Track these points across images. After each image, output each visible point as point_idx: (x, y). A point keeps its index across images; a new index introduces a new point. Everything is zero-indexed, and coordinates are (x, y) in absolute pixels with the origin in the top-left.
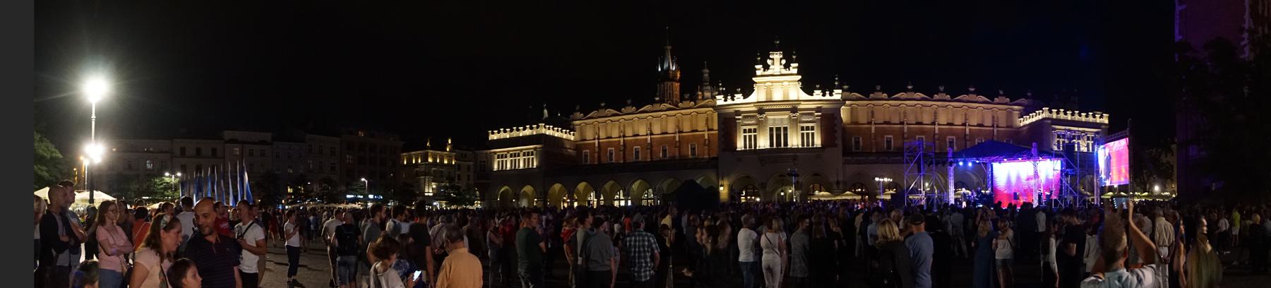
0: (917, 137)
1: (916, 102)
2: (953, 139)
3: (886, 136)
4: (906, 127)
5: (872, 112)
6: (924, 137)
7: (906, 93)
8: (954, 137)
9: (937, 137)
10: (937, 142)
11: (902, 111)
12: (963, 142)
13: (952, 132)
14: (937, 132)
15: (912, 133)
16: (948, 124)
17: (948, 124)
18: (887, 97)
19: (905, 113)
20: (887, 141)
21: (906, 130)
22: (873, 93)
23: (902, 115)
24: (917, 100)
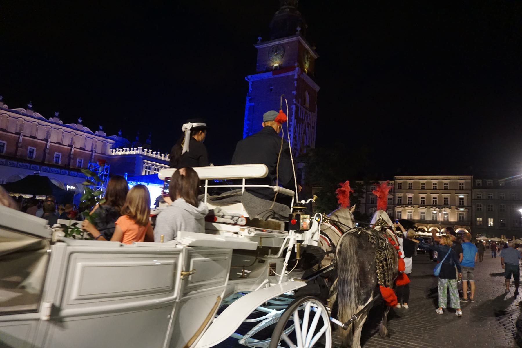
0: (29, 147)
6: (35, 149)
7: (26, 109)
9: (47, 151)
10: (47, 155)
11: (19, 123)
12: (67, 159)
13: (59, 150)
14: (48, 147)
15: (26, 144)
16: (57, 143)
17: (57, 143)
18: (7, 108)
19: (21, 125)
21: (21, 140)
23: (19, 126)
24: (35, 118)
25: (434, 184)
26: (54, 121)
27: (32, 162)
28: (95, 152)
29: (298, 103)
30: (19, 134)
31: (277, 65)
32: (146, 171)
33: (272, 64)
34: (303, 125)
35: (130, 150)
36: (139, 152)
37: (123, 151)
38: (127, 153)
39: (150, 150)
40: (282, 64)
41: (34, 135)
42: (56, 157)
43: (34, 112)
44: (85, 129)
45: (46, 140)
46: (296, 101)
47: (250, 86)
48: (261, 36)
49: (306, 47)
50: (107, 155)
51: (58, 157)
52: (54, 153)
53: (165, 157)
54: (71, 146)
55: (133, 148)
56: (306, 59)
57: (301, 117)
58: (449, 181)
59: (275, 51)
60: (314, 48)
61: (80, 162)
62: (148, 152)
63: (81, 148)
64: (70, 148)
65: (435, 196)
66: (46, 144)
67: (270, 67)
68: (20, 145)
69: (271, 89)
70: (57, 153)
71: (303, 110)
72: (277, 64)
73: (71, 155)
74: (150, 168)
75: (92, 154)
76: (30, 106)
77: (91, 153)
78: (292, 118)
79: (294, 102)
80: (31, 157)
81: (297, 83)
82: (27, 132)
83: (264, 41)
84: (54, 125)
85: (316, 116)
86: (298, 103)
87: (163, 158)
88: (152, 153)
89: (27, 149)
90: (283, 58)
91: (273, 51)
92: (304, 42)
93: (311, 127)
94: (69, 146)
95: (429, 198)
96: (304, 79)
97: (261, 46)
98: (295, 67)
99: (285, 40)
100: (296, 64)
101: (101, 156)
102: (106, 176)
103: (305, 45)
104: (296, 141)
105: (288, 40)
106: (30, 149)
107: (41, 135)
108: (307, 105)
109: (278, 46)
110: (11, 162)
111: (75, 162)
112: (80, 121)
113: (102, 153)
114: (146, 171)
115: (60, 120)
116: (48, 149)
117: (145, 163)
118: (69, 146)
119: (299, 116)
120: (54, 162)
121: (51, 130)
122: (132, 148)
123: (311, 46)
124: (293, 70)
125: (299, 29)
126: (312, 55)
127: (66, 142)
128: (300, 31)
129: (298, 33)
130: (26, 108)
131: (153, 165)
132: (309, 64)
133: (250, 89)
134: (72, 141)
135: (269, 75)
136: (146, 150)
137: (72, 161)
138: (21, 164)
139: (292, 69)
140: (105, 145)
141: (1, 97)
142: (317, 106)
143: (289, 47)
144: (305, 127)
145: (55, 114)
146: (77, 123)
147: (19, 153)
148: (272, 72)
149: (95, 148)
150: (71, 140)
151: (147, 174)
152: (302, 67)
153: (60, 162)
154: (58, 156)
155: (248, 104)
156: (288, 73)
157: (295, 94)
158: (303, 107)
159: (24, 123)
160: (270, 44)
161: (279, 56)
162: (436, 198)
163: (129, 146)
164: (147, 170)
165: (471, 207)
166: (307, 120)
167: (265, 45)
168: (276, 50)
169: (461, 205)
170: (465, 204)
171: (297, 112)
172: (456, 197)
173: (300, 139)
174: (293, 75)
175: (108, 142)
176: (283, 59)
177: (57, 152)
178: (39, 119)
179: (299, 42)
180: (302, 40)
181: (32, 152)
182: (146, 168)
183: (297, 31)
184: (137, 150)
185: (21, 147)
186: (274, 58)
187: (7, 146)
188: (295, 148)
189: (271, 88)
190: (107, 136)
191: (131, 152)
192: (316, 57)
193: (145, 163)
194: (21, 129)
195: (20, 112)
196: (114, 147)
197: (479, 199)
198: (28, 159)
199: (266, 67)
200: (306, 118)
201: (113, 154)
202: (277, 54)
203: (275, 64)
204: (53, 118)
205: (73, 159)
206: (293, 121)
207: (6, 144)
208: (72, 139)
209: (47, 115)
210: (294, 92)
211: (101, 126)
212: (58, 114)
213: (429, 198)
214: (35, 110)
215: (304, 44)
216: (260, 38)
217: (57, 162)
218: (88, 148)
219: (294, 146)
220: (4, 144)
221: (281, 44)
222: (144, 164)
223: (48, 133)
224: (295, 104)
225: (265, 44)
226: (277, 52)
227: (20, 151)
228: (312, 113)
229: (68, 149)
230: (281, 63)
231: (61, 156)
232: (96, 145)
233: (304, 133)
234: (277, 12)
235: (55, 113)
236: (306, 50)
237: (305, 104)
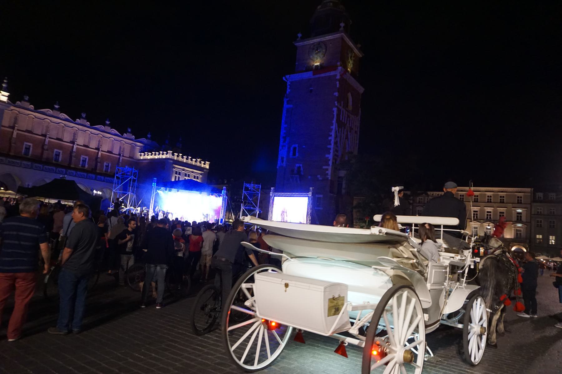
0: (55, 150)
1: (59, 121)
2: (86, 159)
3: (25, 143)
4: (47, 140)
5: (16, 119)
6: (61, 151)
7: (52, 110)
8: (87, 157)
9: (74, 154)
10: (73, 158)
12: (94, 163)
13: (86, 153)
14: (74, 150)
15: (52, 146)
16: (84, 146)
17: (84, 146)
18: (33, 109)
19: (48, 127)
20: (26, 148)
21: (47, 143)
22: (20, 101)
25: (488, 196)
26: (82, 123)
27: (58, 165)
28: (123, 156)
29: (341, 105)
30: (45, 136)
31: (318, 64)
32: (176, 177)
33: (312, 63)
34: (345, 130)
35: (159, 154)
36: (169, 156)
37: (152, 155)
38: (156, 157)
39: (181, 155)
40: (323, 63)
41: (60, 138)
42: (83, 161)
43: (61, 113)
44: (113, 131)
45: (73, 142)
46: (337, 103)
47: (288, 87)
48: (301, 33)
49: (350, 45)
50: (135, 159)
51: (84, 161)
52: (81, 156)
53: (196, 161)
54: (98, 149)
55: (163, 151)
56: (350, 58)
57: (343, 121)
58: (505, 193)
59: (316, 49)
60: (359, 46)
61: (107, 166)
62: (178, 156)
63: (108, 152)
64: (97, 151)
65: (489, 209)
66: (73, 147)
67: (310, 66)
68: (46, 147)
69: (311, 91)
70: (83, 156)
71: (345, 113)
72: (318, 63)
73: (98, 159)
74: (180, 174)
75: (119, 158)
76: (57, 107)
77: (118, 156)
78: (333, 122)
79: (335, 104)
80: (57, 160)
81: (339, 83)
82: (53, 133)
83: (303, 39)
84: (80, 127)
85: (359, 120)
86: (341, 105)
87: (194, 163)
88: (183, 158)
89: (53, 152)
90: (324, 56)
91: (313, 49)
92: (348, 39)
93: (354, 131)
94: (96, 149)
95: (482, 211)
96: (347, 80)
97: (301, 44)
98: (338, 67)
99: (327, 37)
100: (339, 64)
101: (129, 160)
102: (134, 181)
103: (349, 42)
104: (337, 147)
105: (330, 37)
106: (56, 152)
107: (67, 137)
108: (350, 108)
109: (319, 43)
110: (37, 165)
111: (102, 166)
112: (108, 122)
113: (130, 157)
114: (176, 177)
115: (87, 121)
116: (74, 152)
117: (174, 168)
118: (96, 149)
119: (341, 120)
120: (80, 166)
121: (77, 132)
122: (161, 152)
123: (355, 43)
124: (336, 70)
125: (342, 25)
126: (356, 53)
127: (93, 145)
128: (344, 27)
129: (342, 29)
130: (53, 108)
131: (184, 170)
132: (353, 63)
133: (288, 90)
134: (99, 144)
135: (308, 75)
136: (176, 154)
137: (99, 164)
138: (47, 167)
139: (335, 68)
140: (133, 148)
141: (28, 97)
142: (360, 109)
143: (331, 45)
144: (347, 132)
145: (82, 115)
146: (104, 125)
147: (45, 155)
148: (312, 71)
149: (123, 151)
150: (98, 142)
151: (177, 180)
152: (345, 67)
153: (87, 166)
154: (84, 160)
155: (286, 105)
156: (330, 72)
157: (337, 96)
158: (346, 110)
159: (50, 124)
160: (310, 41)
161: (320, 54)
162: (490, 212)
163: (158, 150)
164: (177, 176)
165: (530, 222)
166: (349, 124)
167: (305, 42)
168: (317, 48)
169: (519, 219)
170: (524, 219)
171: (338, 115)
172: (513, 212)
173: (342, 144)
174: (336, 75)
175: (136, 146)
176: (324, 58)
177: (83, 155)
178: (66, 120)
179: (342, 39)
180: (346, 38)
181: (58, 155)
182: (176, 173)
183: (341, 27)
184: (167, 154)
185: (47, 150)
186: (315, 56)
187: (33, 148)
188: (335, 155)
189: (311, 89)
190: (135, 139)
191: (161, 156)
192: (361, 56)
193: (174, 168)
194: (47, 131)
195: (46, 113)
196: (143, 151)
197: (538, 214)
198: (54, 162)
199: (306, 66)
200: (348, 122)
201: (142, 158)
202: (316, 54)
203: (316, 63)
204: (80, 119)
205: (100, 162)
206: (334, 124)
207: (32, 146)
208: (99, 141)
209: (74, 117)
210: (336, 94)
211: (129, 128)
212: (85, 115)
213: (482, 211)
214: (61, 110)
215: (347, 42)
216: (300, 35)
217: (83, 165)
218: (116, 151)
219: (335, 153)
220: (30, 146)
221: (324, 41)
222: (174, 169)
223: (75, 135)
224: (337, 107)
225: (305, 41)
226: (319, 50)
227: (45, 155)
228: (355, 116)
229: (95, 152)
230: (322, 62)
231: (87, 159)
232: (124, 149)
233: (346, 138)
234: (319, 7)
235: (82, 114)
236: (349, 47)
237: (347, 106)
